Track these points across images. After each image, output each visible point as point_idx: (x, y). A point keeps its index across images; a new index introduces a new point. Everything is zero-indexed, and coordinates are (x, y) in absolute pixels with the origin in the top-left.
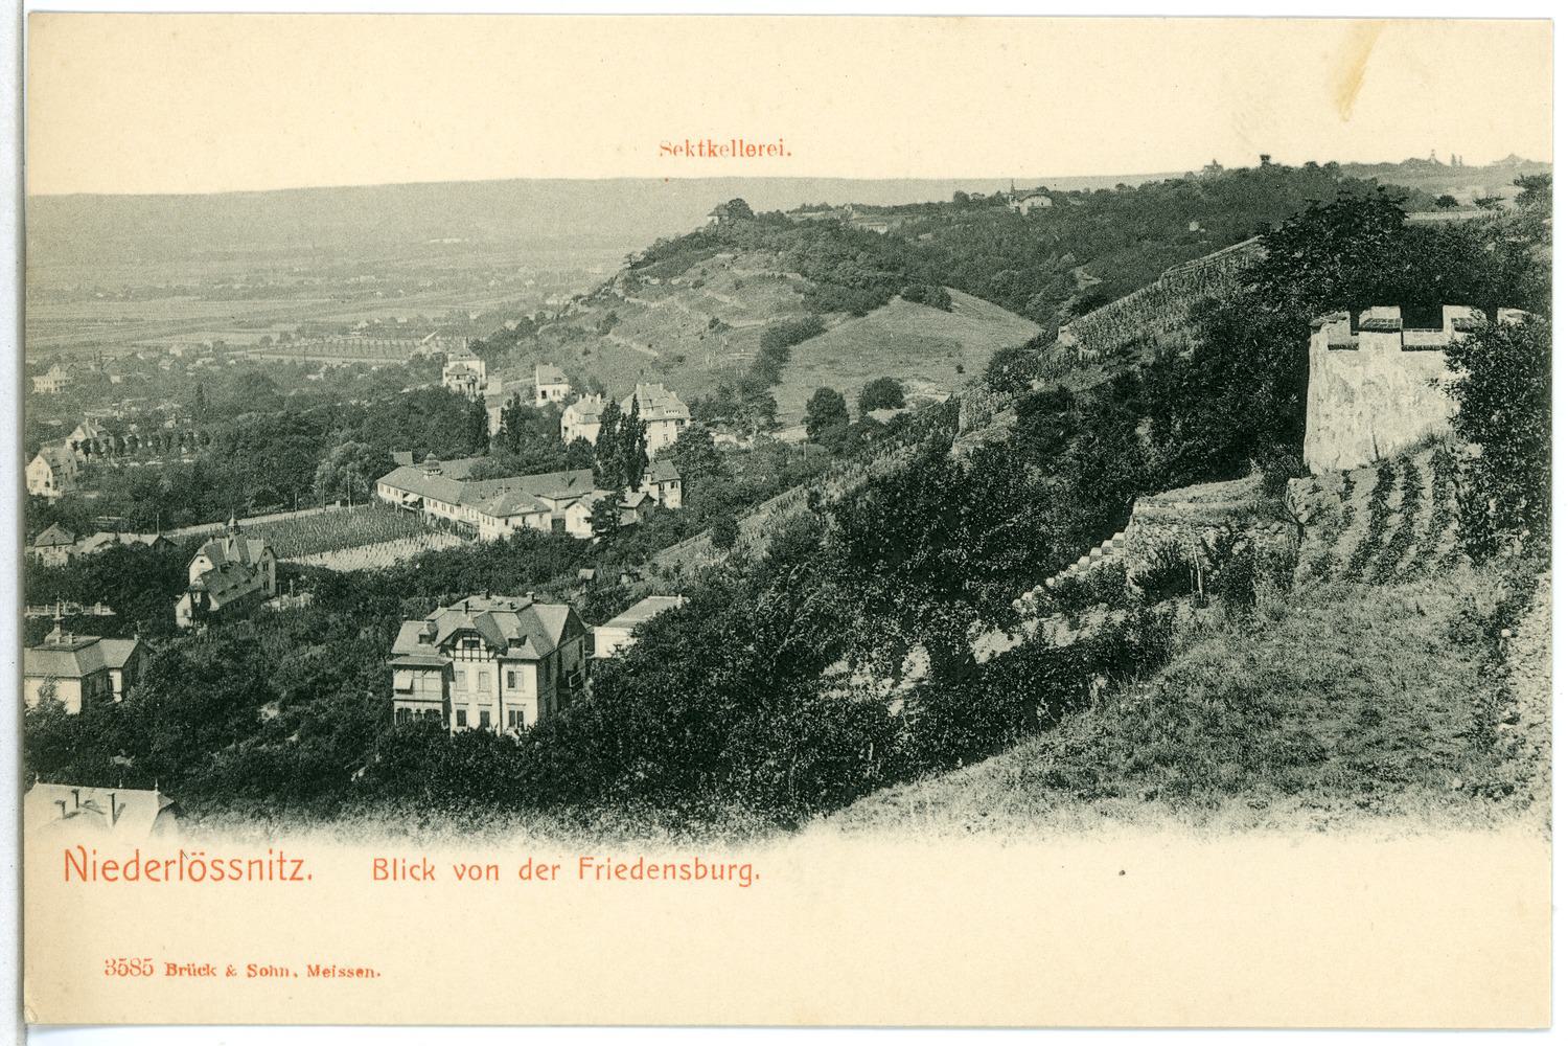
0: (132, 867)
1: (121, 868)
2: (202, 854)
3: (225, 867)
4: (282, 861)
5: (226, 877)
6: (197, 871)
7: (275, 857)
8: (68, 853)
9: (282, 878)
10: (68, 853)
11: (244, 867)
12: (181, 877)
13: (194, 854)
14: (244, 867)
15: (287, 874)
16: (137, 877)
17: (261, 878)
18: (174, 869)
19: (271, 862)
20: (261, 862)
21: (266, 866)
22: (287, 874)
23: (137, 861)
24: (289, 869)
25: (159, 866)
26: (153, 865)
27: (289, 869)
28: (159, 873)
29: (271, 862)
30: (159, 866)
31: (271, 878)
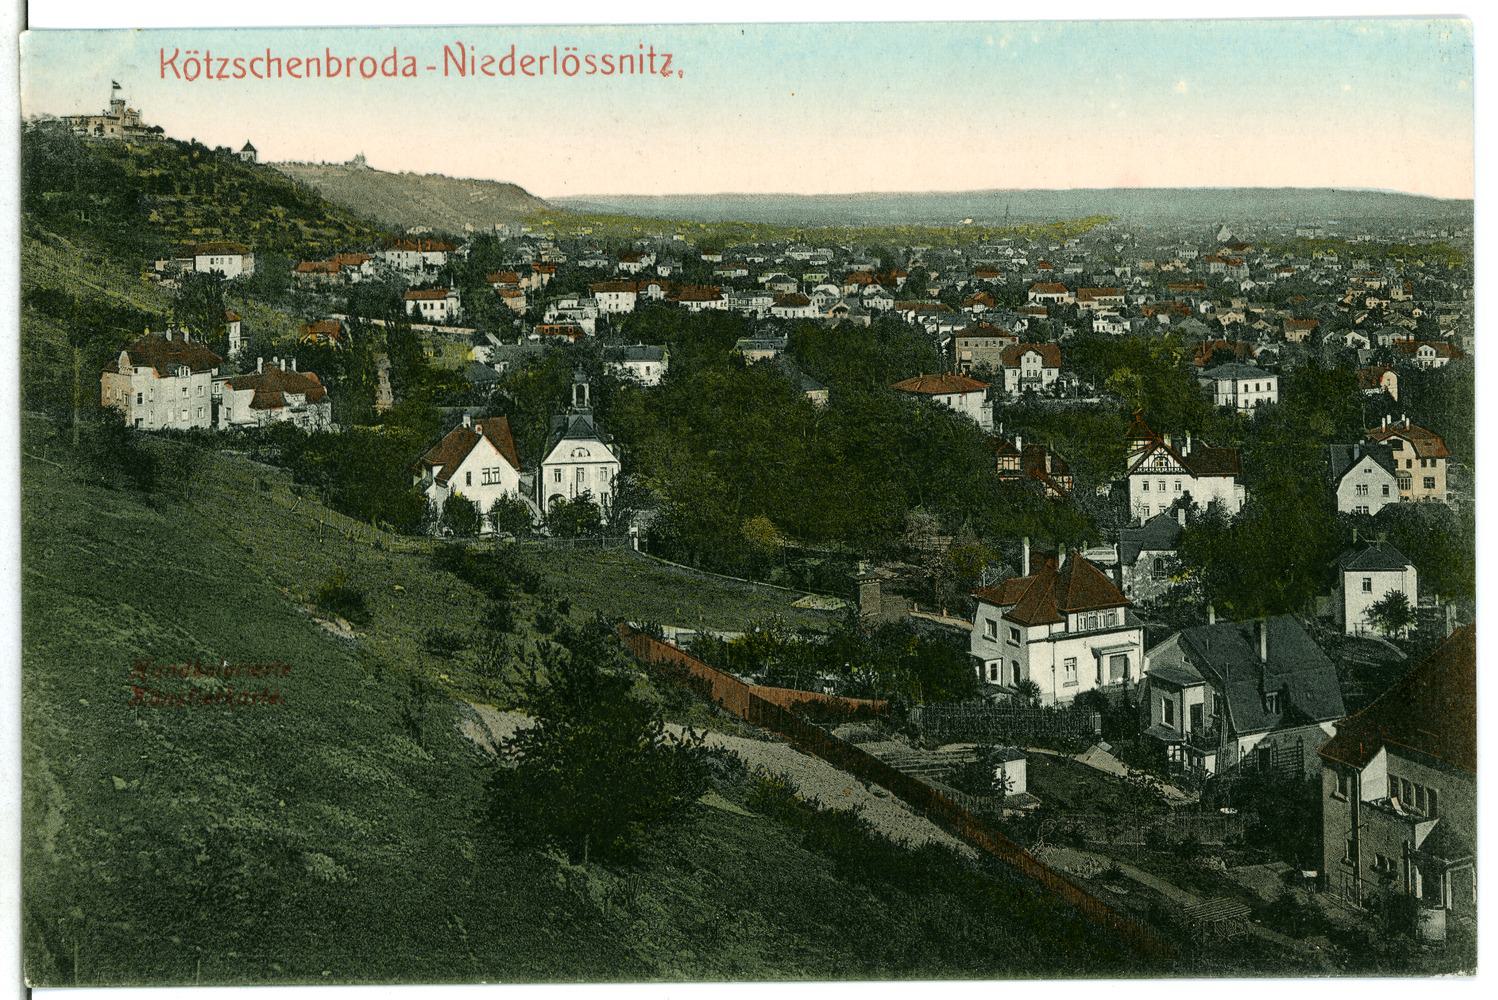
0: (509, 61)
1: (497, 63)
2: (575, 49)
3: (601, 66)
4: (652, 55)
5: (599, 72)
6: (571, 65)
7: (646, 51)
8: (447, 49)
9: (652, 72)
10: (447, 49)
11: (616, 63)
12: (555, 72)
13: (567, 49)
14: (616, 63)
15: (658, 67)
16: (513, 72)
17: (632, 71)
18: (548, 64)
19: (641, 56)
20: (632, 58)
21: (637, 62)
22: (658, 67)
23: (512, 56)
24: (659, 62)
25: (533, 60)
27: (659, 62)
28: (534, 68)
29: (641, 56)
30: (533, 60)
31: (641, 71)
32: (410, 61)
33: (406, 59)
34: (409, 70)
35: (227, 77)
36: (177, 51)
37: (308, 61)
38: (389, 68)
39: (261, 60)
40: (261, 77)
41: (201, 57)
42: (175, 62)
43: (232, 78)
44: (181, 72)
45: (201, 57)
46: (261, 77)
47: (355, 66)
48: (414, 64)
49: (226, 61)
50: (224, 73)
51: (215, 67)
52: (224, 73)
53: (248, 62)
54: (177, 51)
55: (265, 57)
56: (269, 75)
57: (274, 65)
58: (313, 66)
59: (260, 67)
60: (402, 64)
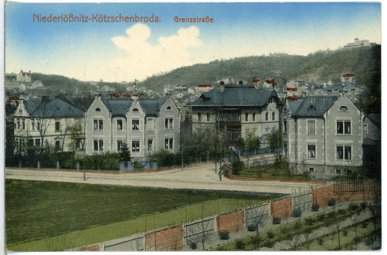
26: (45, 18)
32: (157, 18)
33: (156, 17)
34: (156, 20)
35: (110, 21)
36: (97, 14)
37: (131, 18)
38: (151, 20)
39: (118, 17)
40: (118, 22)
41: (103, 16)
42: (96, 18)
43: (111, 22)
44: (98, 21)
45: (103, 16)
46: (118, 22)
47: (143, 19)
48: (158, 19)
49: (109, 17)
50: (109, 21)
51: (106, 19)
52: (109, 21)
53: (115, 18)
54: (97, 14)
55: (119, 17)
56: (120, 21)
57: (121, 19)
58: (132, 19)
59: (118, 19)
60: (155, 19)
